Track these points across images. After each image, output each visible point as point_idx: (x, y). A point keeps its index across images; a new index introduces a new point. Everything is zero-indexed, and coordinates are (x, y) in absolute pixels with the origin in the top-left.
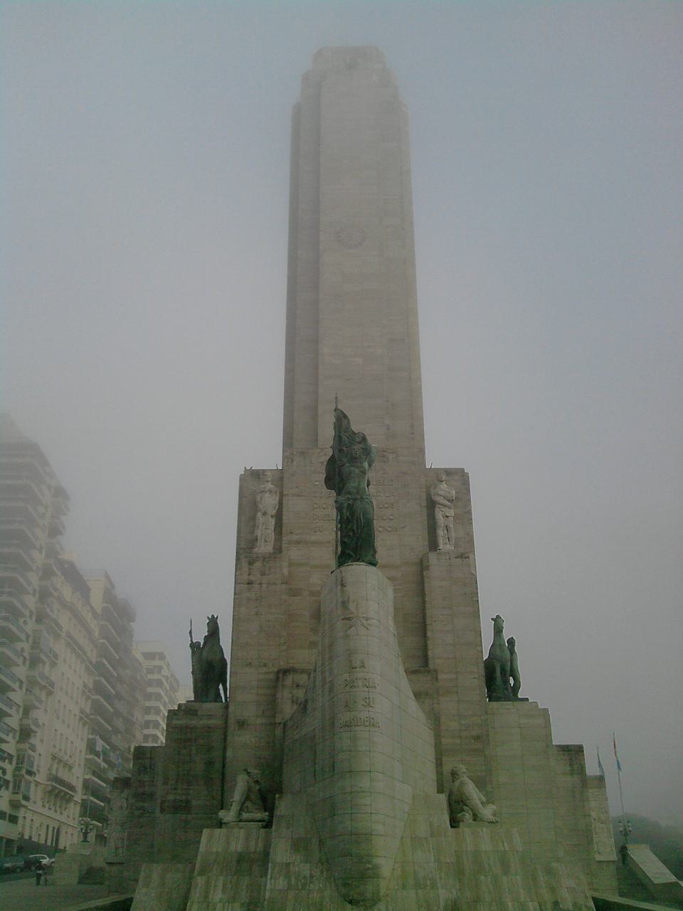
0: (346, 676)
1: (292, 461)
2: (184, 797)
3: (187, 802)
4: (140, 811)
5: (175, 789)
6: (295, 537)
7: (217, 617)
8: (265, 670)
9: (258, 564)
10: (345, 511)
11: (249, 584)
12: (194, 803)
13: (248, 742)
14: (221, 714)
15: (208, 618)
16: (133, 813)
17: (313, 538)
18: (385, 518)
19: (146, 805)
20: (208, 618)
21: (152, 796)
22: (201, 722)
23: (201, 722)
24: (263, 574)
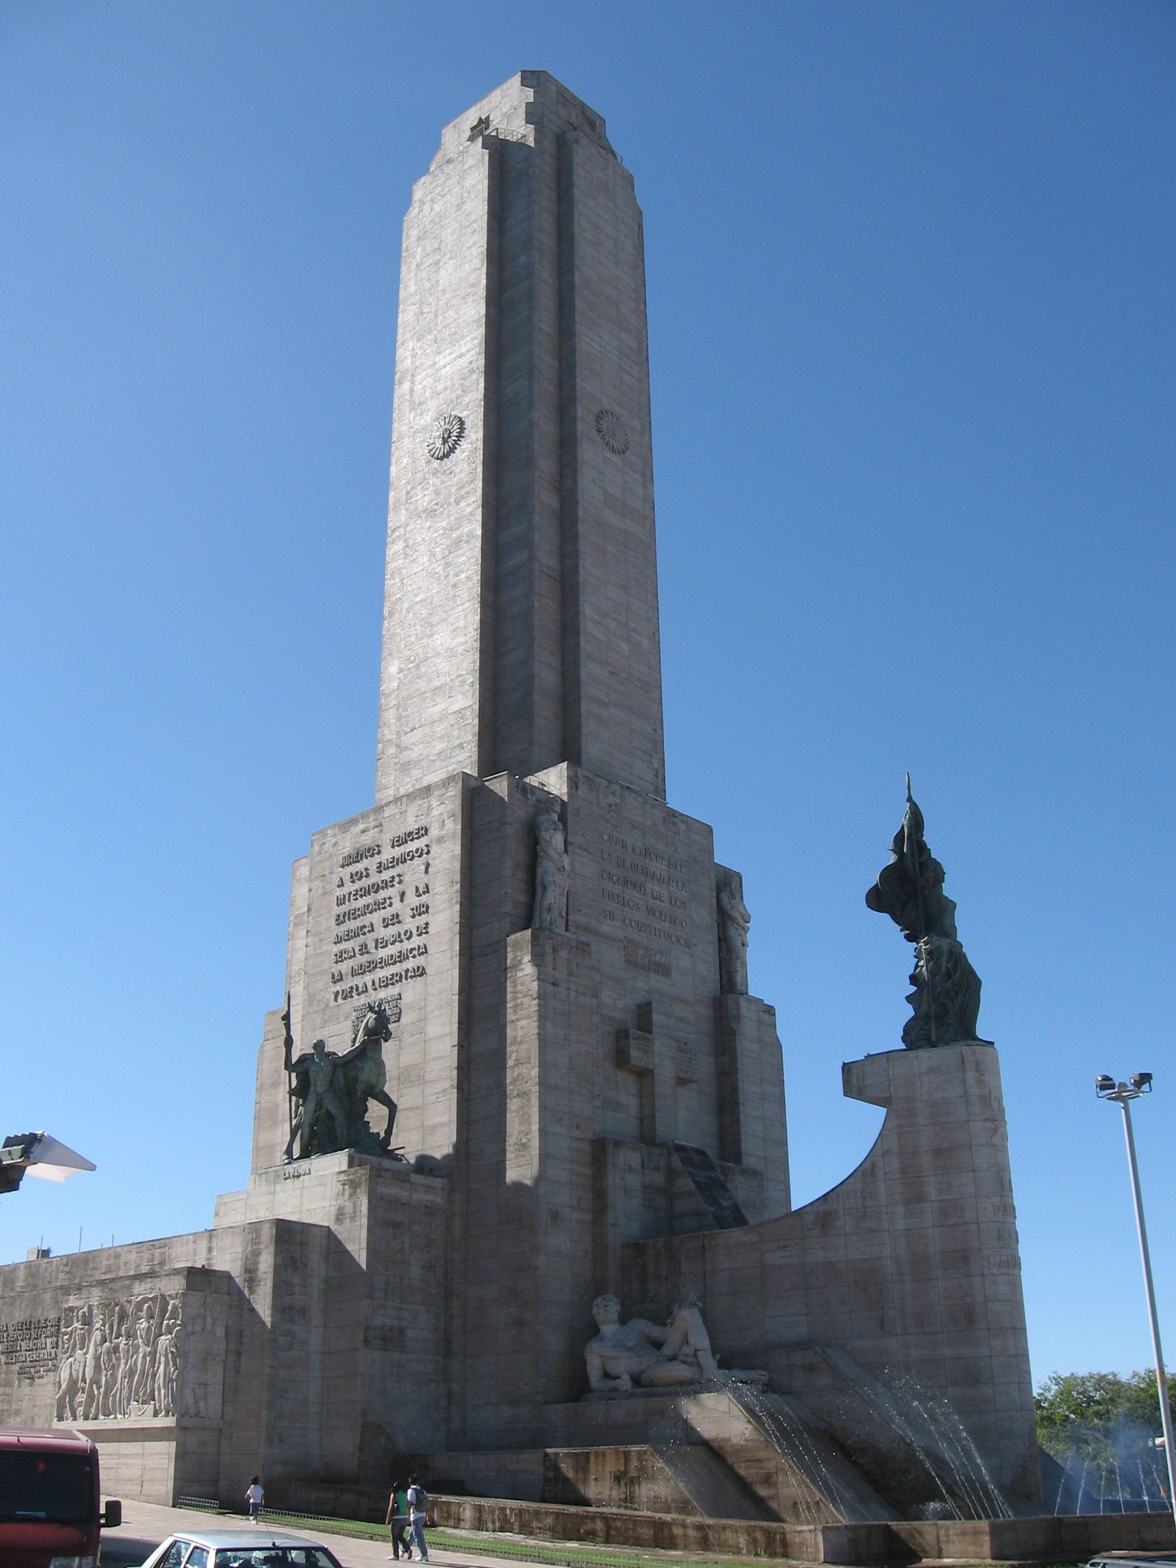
1: (577, 787)
2: (396, 1323)
3: (401, 1331)
4: (289, 1338)
5: (384, 1307)
6: (583, 920)
8: (576, 1133)
9: (563, 954)
10: (944, 959)
11: (554, 984)
12: (410, 1333)
16: (276, 1341)
19: (296, 1328)
21: (304, 1311)
22: (416, 1196)
23: (416, 1196)
24: (570, 974)
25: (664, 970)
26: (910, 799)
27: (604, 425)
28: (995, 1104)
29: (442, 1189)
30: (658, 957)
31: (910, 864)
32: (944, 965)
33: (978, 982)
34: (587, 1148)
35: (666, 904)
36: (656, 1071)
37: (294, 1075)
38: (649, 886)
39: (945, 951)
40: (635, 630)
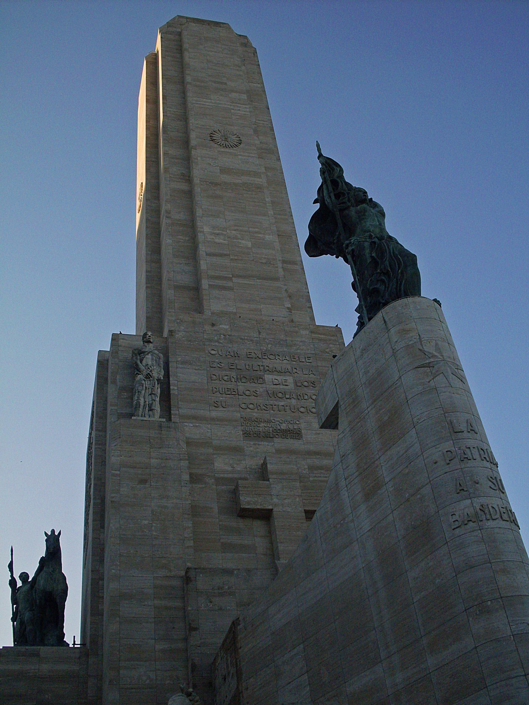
0: (448, 445)
7: (60, 533)
10: (367, 251)
13: (144, 678)
14: (78, 656)
15: (46, 534)
17: (214, 414)
18: (306, 397)
20: (46, 534)
25: (297, 434)
26: (320, 156)
27: (217, 136)
28: (429, 348)
29: (79, 658)
30: (284, 426)
31: (329, 201)
32: (368, 256)
33: (412, 259)
34: (176, 583)
35: (292, 386)
36: (275, 510)
37: (15, 606)
38: (268, 377)
39: (367, 244)
40: (256, 232)
